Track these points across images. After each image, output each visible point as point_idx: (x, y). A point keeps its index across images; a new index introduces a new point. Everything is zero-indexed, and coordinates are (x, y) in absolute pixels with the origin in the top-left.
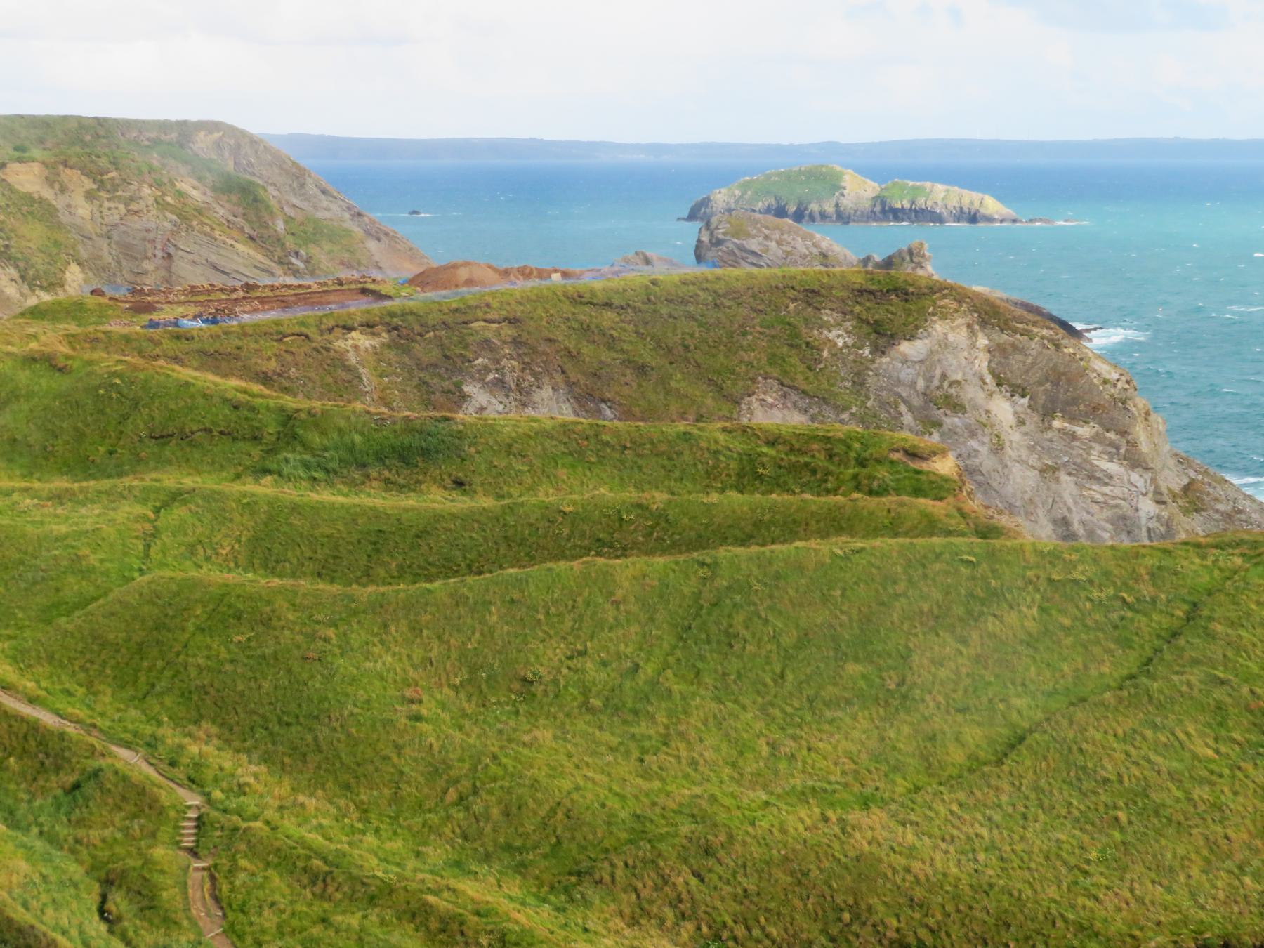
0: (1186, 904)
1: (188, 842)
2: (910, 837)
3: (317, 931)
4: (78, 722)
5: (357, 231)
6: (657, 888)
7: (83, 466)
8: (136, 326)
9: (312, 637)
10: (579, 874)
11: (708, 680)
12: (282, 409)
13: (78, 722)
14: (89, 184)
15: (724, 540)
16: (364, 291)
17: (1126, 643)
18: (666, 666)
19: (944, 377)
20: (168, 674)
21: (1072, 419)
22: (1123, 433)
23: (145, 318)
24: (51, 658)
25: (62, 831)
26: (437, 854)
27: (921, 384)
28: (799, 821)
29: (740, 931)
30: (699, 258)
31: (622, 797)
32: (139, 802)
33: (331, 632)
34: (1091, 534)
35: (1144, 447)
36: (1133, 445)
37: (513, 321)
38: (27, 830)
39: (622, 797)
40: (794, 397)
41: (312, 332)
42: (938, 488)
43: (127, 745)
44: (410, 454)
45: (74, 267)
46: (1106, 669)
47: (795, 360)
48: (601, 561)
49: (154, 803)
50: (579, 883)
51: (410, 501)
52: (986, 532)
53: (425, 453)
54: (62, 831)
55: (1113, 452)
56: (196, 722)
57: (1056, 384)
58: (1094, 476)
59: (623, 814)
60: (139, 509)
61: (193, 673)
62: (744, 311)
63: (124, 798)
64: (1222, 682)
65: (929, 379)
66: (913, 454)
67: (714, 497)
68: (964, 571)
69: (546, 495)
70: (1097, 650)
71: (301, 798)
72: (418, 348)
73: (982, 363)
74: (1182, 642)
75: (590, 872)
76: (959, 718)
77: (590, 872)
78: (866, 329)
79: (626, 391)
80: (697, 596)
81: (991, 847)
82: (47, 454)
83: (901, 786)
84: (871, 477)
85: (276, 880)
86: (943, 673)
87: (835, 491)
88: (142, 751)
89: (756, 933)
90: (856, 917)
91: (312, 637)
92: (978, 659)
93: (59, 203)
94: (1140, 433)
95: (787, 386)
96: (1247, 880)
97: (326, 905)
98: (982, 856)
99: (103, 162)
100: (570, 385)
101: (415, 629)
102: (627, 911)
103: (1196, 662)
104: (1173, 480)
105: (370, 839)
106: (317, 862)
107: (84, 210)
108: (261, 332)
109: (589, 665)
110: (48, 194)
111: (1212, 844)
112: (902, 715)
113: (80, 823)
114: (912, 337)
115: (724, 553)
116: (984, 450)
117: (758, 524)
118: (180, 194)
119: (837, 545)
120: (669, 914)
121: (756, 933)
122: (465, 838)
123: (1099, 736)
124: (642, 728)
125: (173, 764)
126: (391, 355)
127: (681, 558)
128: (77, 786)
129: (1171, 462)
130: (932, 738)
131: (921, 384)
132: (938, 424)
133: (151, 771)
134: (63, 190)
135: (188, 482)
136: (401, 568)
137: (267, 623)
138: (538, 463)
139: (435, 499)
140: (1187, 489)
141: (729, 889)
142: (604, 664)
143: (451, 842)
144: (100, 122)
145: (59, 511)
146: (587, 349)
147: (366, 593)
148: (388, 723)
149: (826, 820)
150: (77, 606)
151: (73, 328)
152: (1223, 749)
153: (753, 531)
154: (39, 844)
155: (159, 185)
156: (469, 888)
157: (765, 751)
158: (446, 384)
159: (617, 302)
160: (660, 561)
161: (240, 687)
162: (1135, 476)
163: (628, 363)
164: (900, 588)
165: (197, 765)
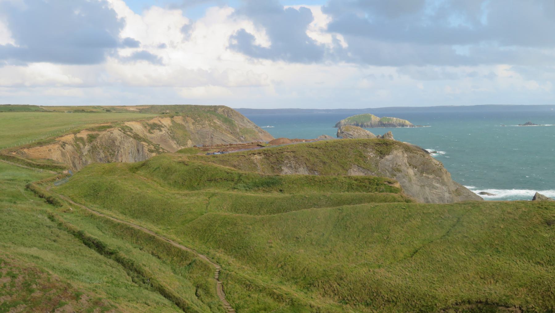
0: (459, 291)
1: (217, 277)
2: (390, 275)
3: (248, 298)
4: (191, 248)
5: (257, 131)
6: (329, 288)
7: (192, 188)
8: (204, 154)
9: (246, 228)
10: (310, 284)
11: (341, 237)
12: (239, 174)
13: (191, 248)
14: (193, 121)
15: (344, 204)
16: (258, 145)
17: (442, 228)
18: (331, 234)
19: (396, 164)
20: (212, 237)
21: (428, 174)
22: (441, 177)
23: (206, 152)
24: (184, 233)
25: (187, 275)
26: (276, 280)
27: (391, 165)
28: (363, 271)
29: (349, 298)
30: (338, 136)
31: (321, 266)
32: (206, 268)
33: (251, 227)
34: (433, 201)
35: (446, 180)
36: (443, 180)
37: (293, 152)
38: (178, 274)
39: (321, 266)
40: (361, 169)
41: (246, 155)
42: (396, 191)
43: (202, 254)
44: (269, 184)
45: (190, 140)
46: (437, 234)
47: (361, 160)
48: (315, 209)
49: (208, 268)
50: (310, 286)
51: (269, 195)
52: (407, 201)
53: (273, 183)
54: (187, 275)
56: (219, 248)
57: (424, 165)
59: (321, 270)
60: (205, 198)
61: (218, 236)
62: (349, 149)
63: (201, 267)
64: (466, 237)
65: (393, 165)
66: (390, 183)
67: (342, 193)
68: (403, 210)
69: (302, 193)
70: (435, 230)
71: (243, 266)
72: (271, 159)
73: (406, 160)
74: (456, 227)
75: (313, 284)
76: (402, 246)
77: (313, 284)
78: (378, 153)
79: (321, 168)
80: (338, 217)
81: (410, 277)
82: (183, 185)
83: (388, 263)
84: (380, 188)
85: (238, 286)
86: (398, 235)
87: (371, 192)
88: (206, 255)
89: (353, 298)
90: (377, 294)
91: (246, 228)
92: (406, 232)
93: (186, 125)
94: (444, 177)
95: (359, 166)
96: (474, 285)
97: (249, 292)
98: (408, 279)
99: (196, 116)
100: (307, 167)
101: (271, 226)
102: (322, 293)
103: (460, 232)
104: (453, 188)
105: (260, 276)
106: (247, 282)
107: (192, 127)
109: (312, 234)
110: (183, 123)
111: (465, 277)
112: (388, 246)
113: (191, 273)
114: (388, 155)
115: (345, 207)
116: (407, 181)
117: (353, 200)
118: (215, 123)
119: (372, 204)
120: (332, 294)
121: (353, 298)
122: (283, 276)
123: (436, 250)
124: (325, 249)
125: (213, 258)
126: (265, 160)
127: (334, 208)
128: (190, 264)
129: (452, 184)
130: (395, 251)
131: (391, 165)
132: (395, 175)
133: (208, 260)
134: (187, 122)
135: (216, 191)
136: (267, 211)
137: (235, 224)
138: (300, 185)
139: (275, 194)
140: (456, 190)
141: (346, 288)
142: (316, 234)
143: (279, 277)
144: (196, 106)
145: (186, 198)
146: (311, 158)
147: (258, 217)
148: (264, 248)
149: (370, 271)
150: (191, 221)
151: (189, 155)
152: (467, 253)
153: (351, 202)
154: (181, 278)
155: (210, 121)
156: (284, 288)
157: (355, 254)
158: (278, 167)
159: (318, 147)
160: (329, 209)
161: (229, 240)
162: (444, 187)
163: (321, 161)
164: (387, 214)
165: (219, 259)
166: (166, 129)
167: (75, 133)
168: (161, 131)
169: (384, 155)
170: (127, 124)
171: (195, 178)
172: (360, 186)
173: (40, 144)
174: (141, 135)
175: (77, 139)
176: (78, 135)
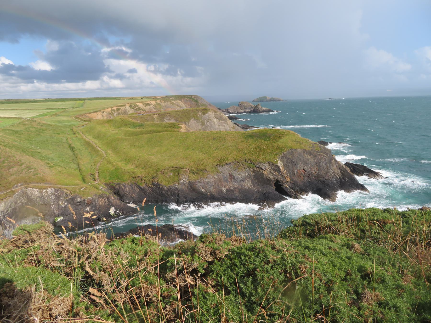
44: (141, 126)
58: (224, 126)
108: (146, 115)
172: (169, 126)
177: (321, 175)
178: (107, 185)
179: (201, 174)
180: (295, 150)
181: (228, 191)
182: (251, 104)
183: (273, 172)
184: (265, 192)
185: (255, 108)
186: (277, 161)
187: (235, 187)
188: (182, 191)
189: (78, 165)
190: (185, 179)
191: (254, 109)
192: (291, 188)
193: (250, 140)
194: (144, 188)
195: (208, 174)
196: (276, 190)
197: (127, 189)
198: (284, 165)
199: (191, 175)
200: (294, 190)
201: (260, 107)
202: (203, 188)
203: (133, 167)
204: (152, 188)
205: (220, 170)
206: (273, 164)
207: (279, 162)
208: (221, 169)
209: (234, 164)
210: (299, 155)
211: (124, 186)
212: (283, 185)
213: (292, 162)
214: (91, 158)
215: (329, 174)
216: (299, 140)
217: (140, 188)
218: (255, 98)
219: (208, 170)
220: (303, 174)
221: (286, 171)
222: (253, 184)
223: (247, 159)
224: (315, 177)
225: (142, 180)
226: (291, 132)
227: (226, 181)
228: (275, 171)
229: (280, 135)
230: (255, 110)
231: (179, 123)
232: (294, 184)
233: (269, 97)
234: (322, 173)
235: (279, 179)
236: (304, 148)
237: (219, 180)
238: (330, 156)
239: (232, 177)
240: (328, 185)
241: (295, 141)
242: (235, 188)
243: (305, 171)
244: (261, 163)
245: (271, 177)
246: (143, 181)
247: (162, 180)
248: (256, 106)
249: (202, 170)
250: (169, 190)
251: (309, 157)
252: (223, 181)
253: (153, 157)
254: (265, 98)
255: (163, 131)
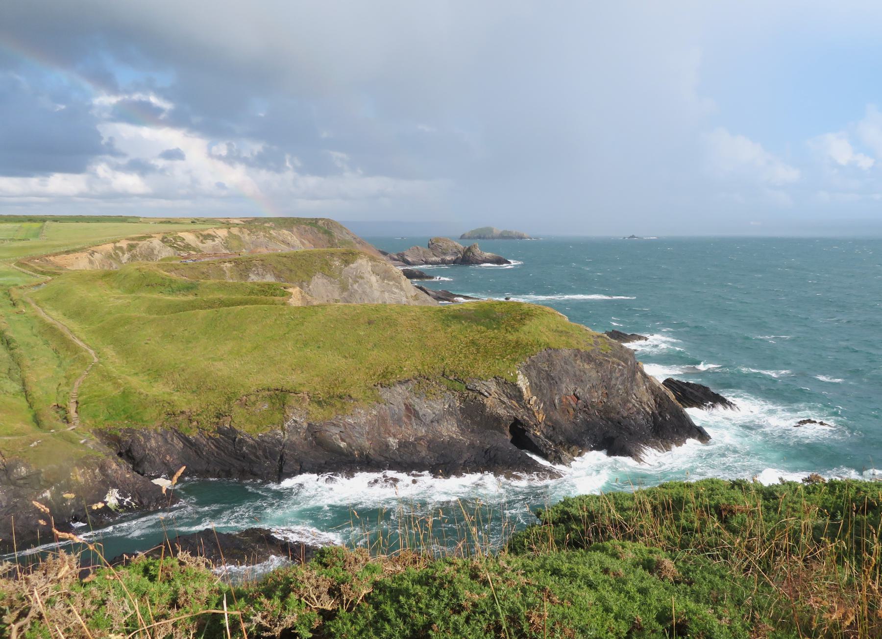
4: (87, 345)
7: (133, 292)
44: (189, 288)
53: (192, 288)
55: (397, 287)
69: (211, 296)
73: (369, 269)
94: (403, 283)
95: (324, 274)
107: (247, 238)
108: (204, 263)
124: (190, 345)
139: (191, 297)
146: (279, 266)
166: (220, 239)
167: (114, 242)
168: (214, 240)
169: (349, 264)
170: (180, 234)
171: (146, 282)
172: (260, 291)
173: (68, 252)
174: (193, 245)
175: (116, 248)
176: (118, 245)
177: (614, 408)
178: (100, 433)
179: (339, 405)
180: (556, 350)
181: (403, 445)
182: (456, 244)
183: (505, 400)
184: (489, 446)
185: (465, 253)
186: (516, 376)
187: (420, 435)
188: (292, 446)
189: (24, 384)
190: (299, 417)
191: (464, 256)
192: (546, 437)
193: (455, 327)
194: (196, 439)
195: (355, 407)
196: (512, 441)
197: (153, 443)
198: (531, 385)
199: (314, 409)
200: (554, 441)
201: (477, 251)
202: (343, 440)
203: (168, 390)
204: (215, 440)
205: (385, 397)
206: (505, 383)
207: (520, 377)
208: (386, 394)
209: (416, 382)
210: (565, 363)
211: (144, 436)
212: (529, 431)
213: (549, 377)
214: (59, 366)
215: (631, 406)
216: (564, 329)
217: (186, 440)
218: (467, 230)
219: (354, 396)
220: (574, 405)
221: (535, 398)
222: (462, 430)
223: (447, 370)
224: (599, 411)
225: (191, 421)
226: (548, 309)
227: (398, 421)
228: (510, 397)
229: (523, 315)
230: (466, 259)
231: (286, 284)
232: (554, 426)
233: (498, 229)
234: (615, 402)
235: (520, 417)
236: (576, 346)
237: (382, 419)
238: (632, 366)
239: (411, 411)
240: (627, 429)
241: (556, 331)
242: (418, 439)
243: (578, 398)
244: (480, 379)
245: (501, 411)
246: (195, 423)
247: (243, 420)
248: (469, 249)
249: (341, 397)
250: (260, 444)
251: (586, 366)
252: (390, 422)
253: (219, 365)
254: (490, 230)
255: (246, 304)
